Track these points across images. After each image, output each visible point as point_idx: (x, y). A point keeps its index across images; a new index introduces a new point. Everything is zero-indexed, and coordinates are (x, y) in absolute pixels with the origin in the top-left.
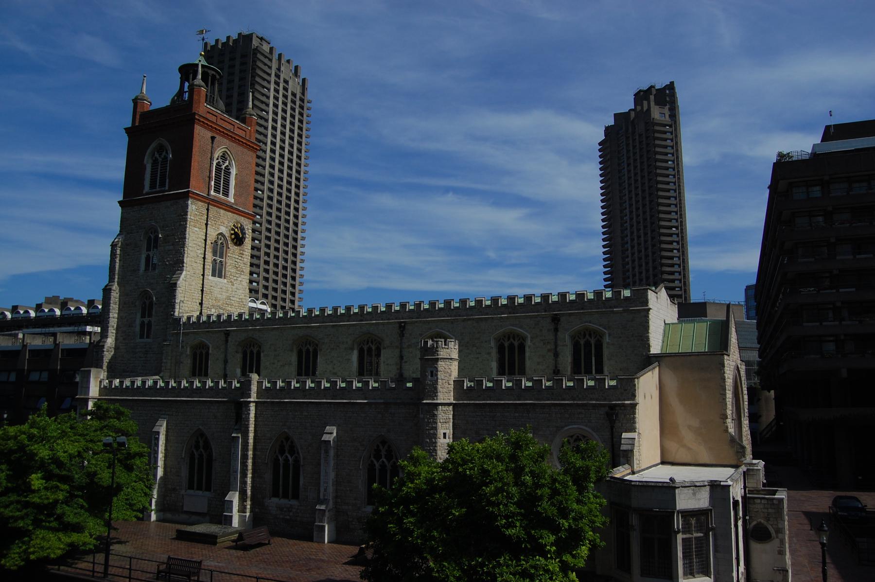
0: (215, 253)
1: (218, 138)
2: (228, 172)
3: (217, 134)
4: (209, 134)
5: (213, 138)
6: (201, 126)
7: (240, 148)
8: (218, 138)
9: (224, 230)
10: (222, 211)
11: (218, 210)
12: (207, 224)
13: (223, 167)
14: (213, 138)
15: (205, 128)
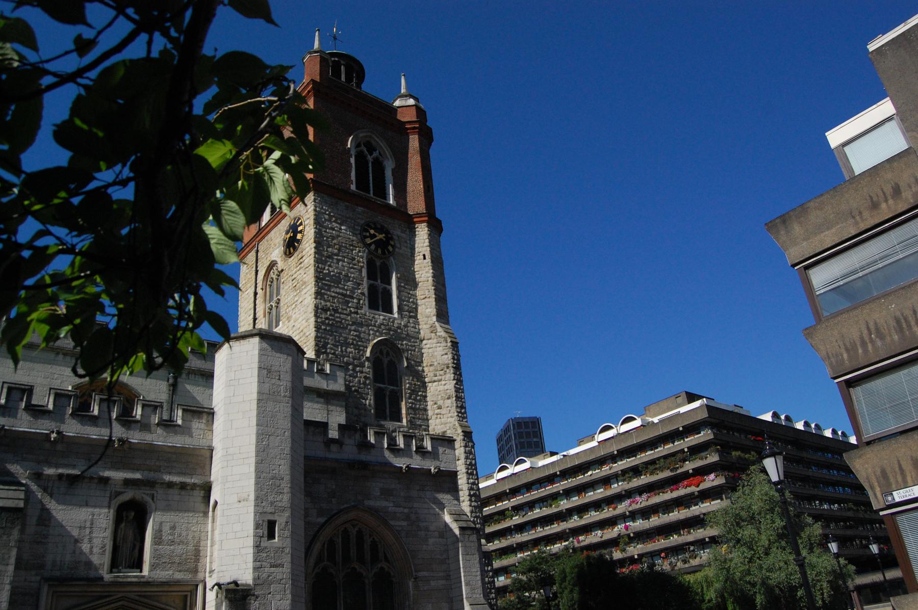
11: (270, 235)
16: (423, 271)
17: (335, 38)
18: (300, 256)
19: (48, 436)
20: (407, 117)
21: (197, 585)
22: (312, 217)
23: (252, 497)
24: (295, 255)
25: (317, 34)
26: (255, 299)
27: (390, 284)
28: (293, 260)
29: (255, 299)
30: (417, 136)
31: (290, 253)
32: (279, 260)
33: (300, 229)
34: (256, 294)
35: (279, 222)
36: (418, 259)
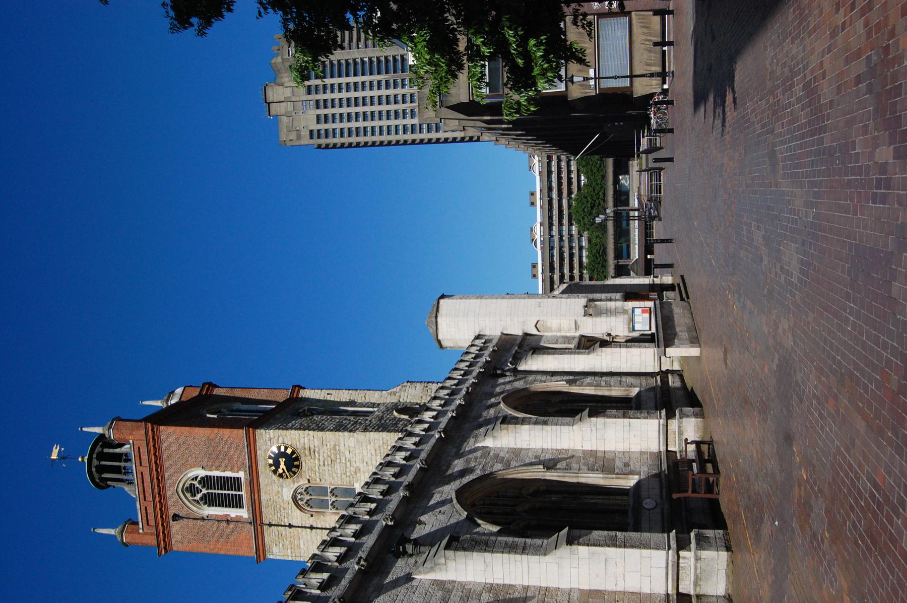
0: (323, 504)
1: (172, 510)
2: (206, 481)
3: (167, 509)
4: (175, 526)
5: (176, 517)
6: (170, 539)
7: (166, 462)
8: (172, 510)
9: (287, 493)
10: (264, 497)
11: (263, 503)
12: (290, 526)
13: (204, 491)
14: (176, 517)
15: (169, 531)
16: (343, 396)
17: (64, 458)
18: (307, 452)
19: (487, 361)
20: (195, 393)
21: (583, 336)
22: (281, 432)
23: (539, 300)
24: (303, 459)
25: (85, 429)
26: (317, 528)
27: (347, 411)
28: (307, 463)
29: (317, 528)
30: (216, 389)
31: (298, 467)
32: (296, 485)
33: (282, 449)
34: (312, 528)
35: (258, 485)
36: (329, 398)
